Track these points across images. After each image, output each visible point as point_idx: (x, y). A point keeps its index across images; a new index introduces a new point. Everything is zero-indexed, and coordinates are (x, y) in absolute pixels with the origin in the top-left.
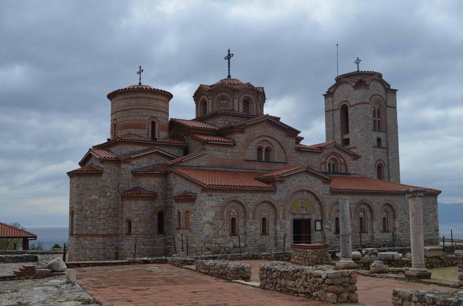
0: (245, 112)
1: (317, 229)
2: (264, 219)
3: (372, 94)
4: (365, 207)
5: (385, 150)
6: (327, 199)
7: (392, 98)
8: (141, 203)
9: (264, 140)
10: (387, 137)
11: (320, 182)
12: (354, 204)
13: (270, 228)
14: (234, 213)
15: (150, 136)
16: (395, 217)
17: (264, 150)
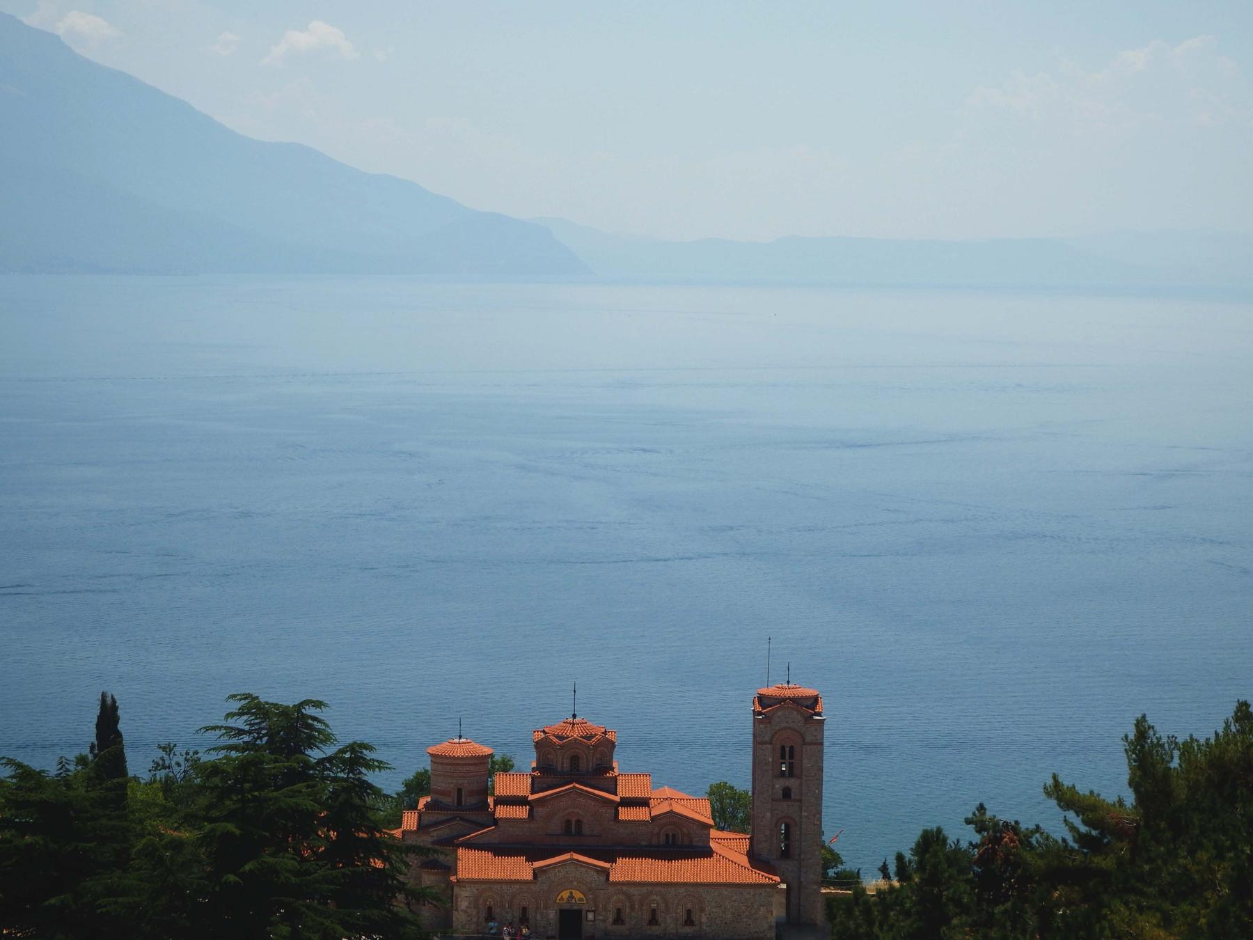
0: (575, 768)
1: (588, 919)
2: (524, 909)
3: (778, 728)
4: (658, 898)
5: (797, 804)
6: (601, 891)
7: (816, 730)
8: (432, 878)
9: (574, 812)
10: (801, 784)
11: (592, 873)
12: (639, 895)
13: (530, 917)
14: (490, 902)
15: (456, 805)
16: (702, 910)
17: (574, 823)
